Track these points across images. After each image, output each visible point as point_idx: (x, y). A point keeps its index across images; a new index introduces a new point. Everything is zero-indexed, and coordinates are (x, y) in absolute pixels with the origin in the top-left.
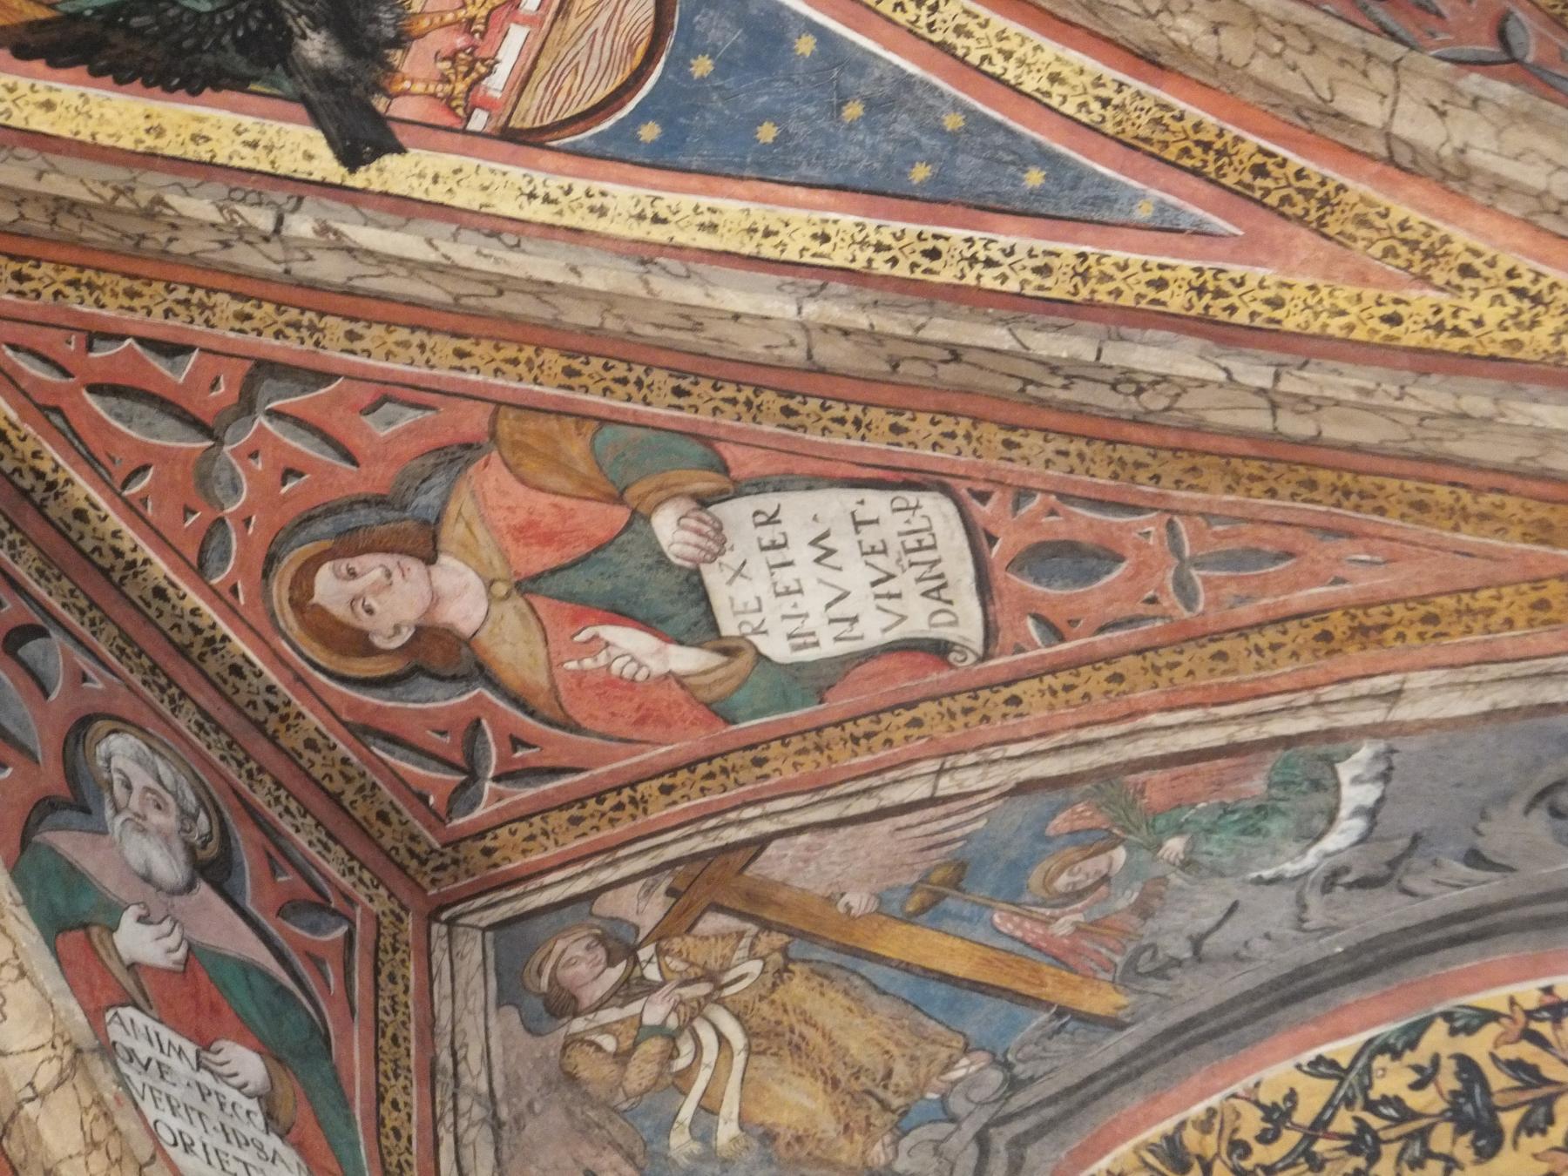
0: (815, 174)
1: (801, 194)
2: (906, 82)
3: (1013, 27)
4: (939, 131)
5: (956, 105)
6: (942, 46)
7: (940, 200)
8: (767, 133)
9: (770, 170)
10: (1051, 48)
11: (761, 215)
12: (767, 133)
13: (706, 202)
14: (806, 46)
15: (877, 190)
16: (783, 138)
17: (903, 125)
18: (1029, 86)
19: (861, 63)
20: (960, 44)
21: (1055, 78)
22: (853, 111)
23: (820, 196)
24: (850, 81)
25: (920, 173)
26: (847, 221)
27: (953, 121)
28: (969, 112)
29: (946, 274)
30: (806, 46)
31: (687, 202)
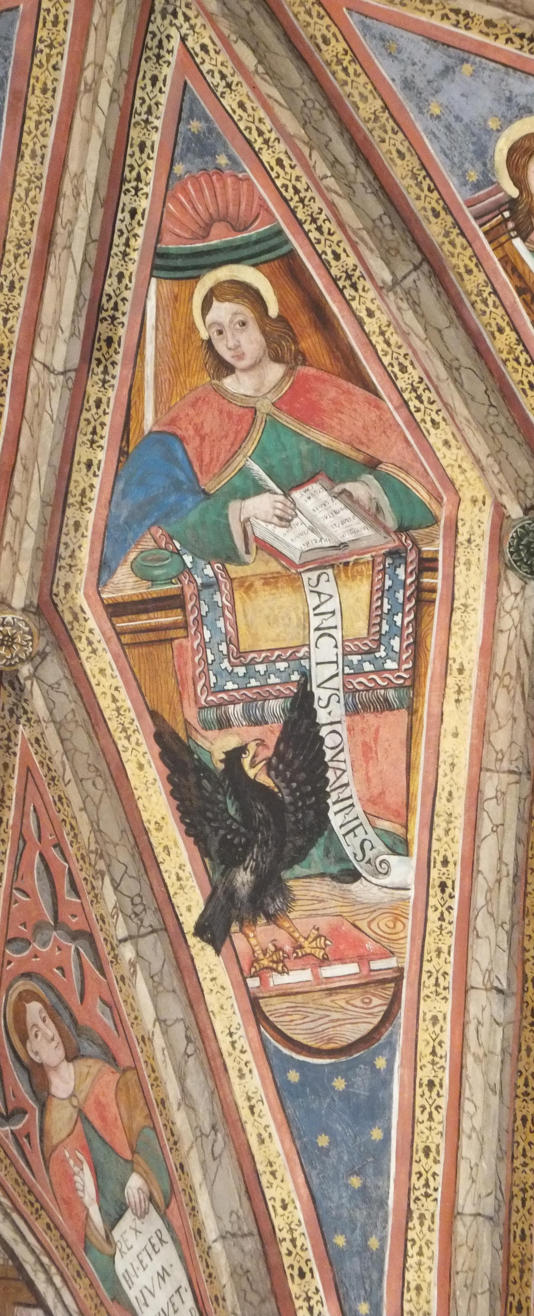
0: (315, 1181)
1: (301, 1179)
2: (383, 1203)
3: (435, 1248)
4: (366, 1238)
5: (383, 1240)
6: (409, 1212)
7: (331, 1259)
8: (323, 1141)
9: (306, 1155)
10: (433, 1277)
11: (281, 1164)
12: (323, 1141)
13: (273, 1129)
14: (377, 1134)
15: (322, 1223)
16: (325, 1152)
17: (360, 1216)
18: (409, 1276)
19: (382, 1172)
20: (415, 1222)
21: (418, 1288)
22: (356, 1182)
23: (305, 1191)
24: (370, 1171)
25: (340, 1241)
26: (299, 1214)
27: (374, 1243)
28: (382, 1249)
29: (295, 1288)
30: (377, 1134)
31: (268, 1119)
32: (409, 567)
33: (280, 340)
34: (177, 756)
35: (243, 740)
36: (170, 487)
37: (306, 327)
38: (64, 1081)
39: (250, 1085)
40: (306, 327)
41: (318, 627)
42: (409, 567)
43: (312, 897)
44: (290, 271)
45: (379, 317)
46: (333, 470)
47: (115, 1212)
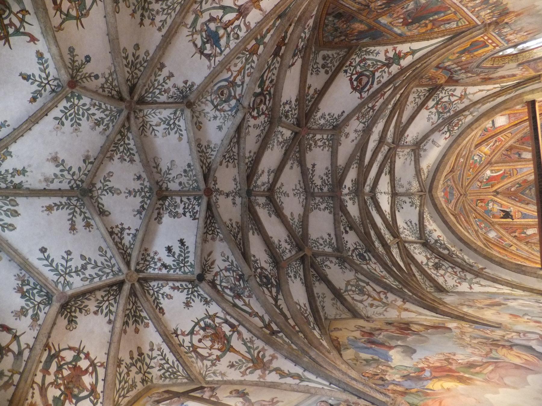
32: (494, 202)
33: (482, 202)
34: (502, 218)
35: (502, 214)
36: (488, 212)
37: (482, 201)
38: (516, 234)
39: (523, 220)
40: (482, 201)
41: (496, 208)
42: (494, 202)
43: (512, 214)
44: (478, 200)
45: (482, 197)
46: (488, 203)
47: (525, 233)
